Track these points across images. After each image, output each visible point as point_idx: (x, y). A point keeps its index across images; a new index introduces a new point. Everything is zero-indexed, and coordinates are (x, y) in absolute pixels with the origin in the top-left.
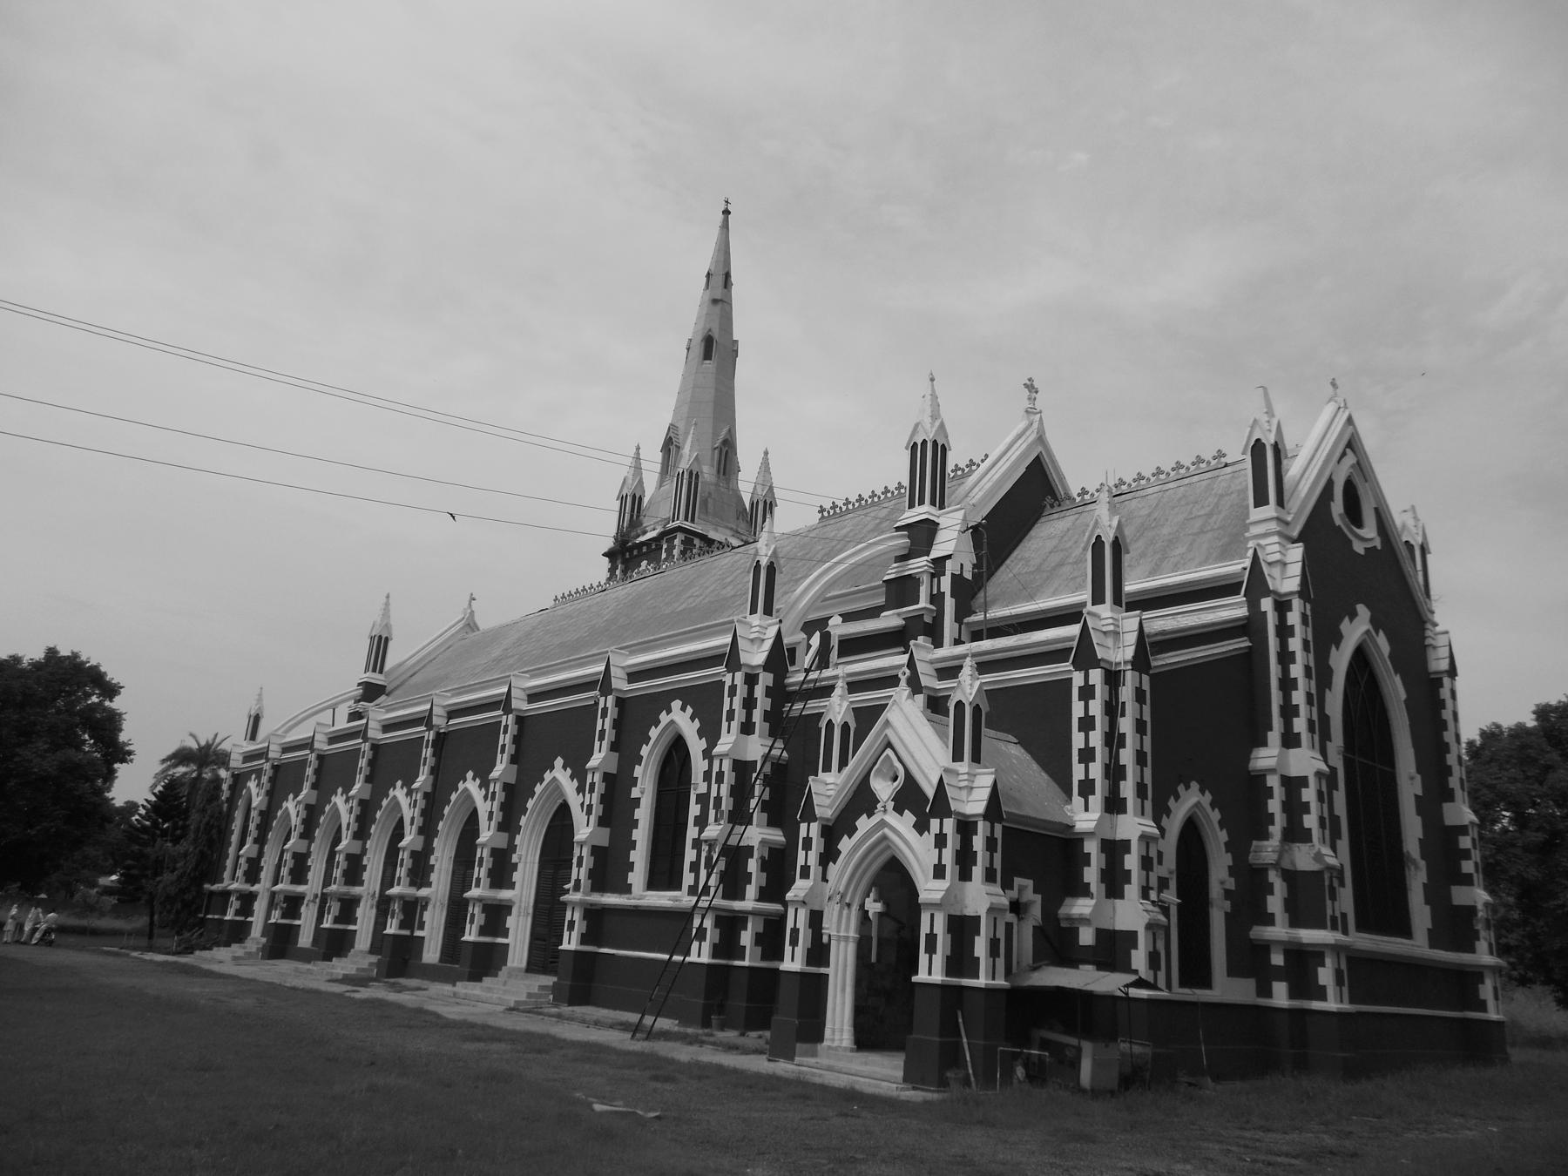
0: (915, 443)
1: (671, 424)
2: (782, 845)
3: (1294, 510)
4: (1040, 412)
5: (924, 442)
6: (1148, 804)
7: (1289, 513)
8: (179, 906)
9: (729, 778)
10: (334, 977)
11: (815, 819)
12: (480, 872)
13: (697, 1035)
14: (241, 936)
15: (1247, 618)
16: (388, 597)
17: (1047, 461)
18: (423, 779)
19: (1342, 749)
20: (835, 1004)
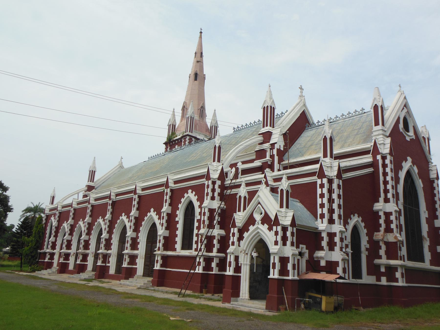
0: (265, 107)
1: (184, 102)
2: (224, 235)
3: (388, 127)
4: (304, 96)
5: (268, 106)
6: (342, 221)
7: (386, 128)
8: (30, 257)
9: (207, 214)
10: (81, 279)
11: (236, 227)
12: (128, 245)
13: (199, 295)
14: (50, 267)
15: (373, 162)
16: (95, 158)
17: (307, 112)
18: (108, 216)
19: (403, 203)
20: (243, 285)
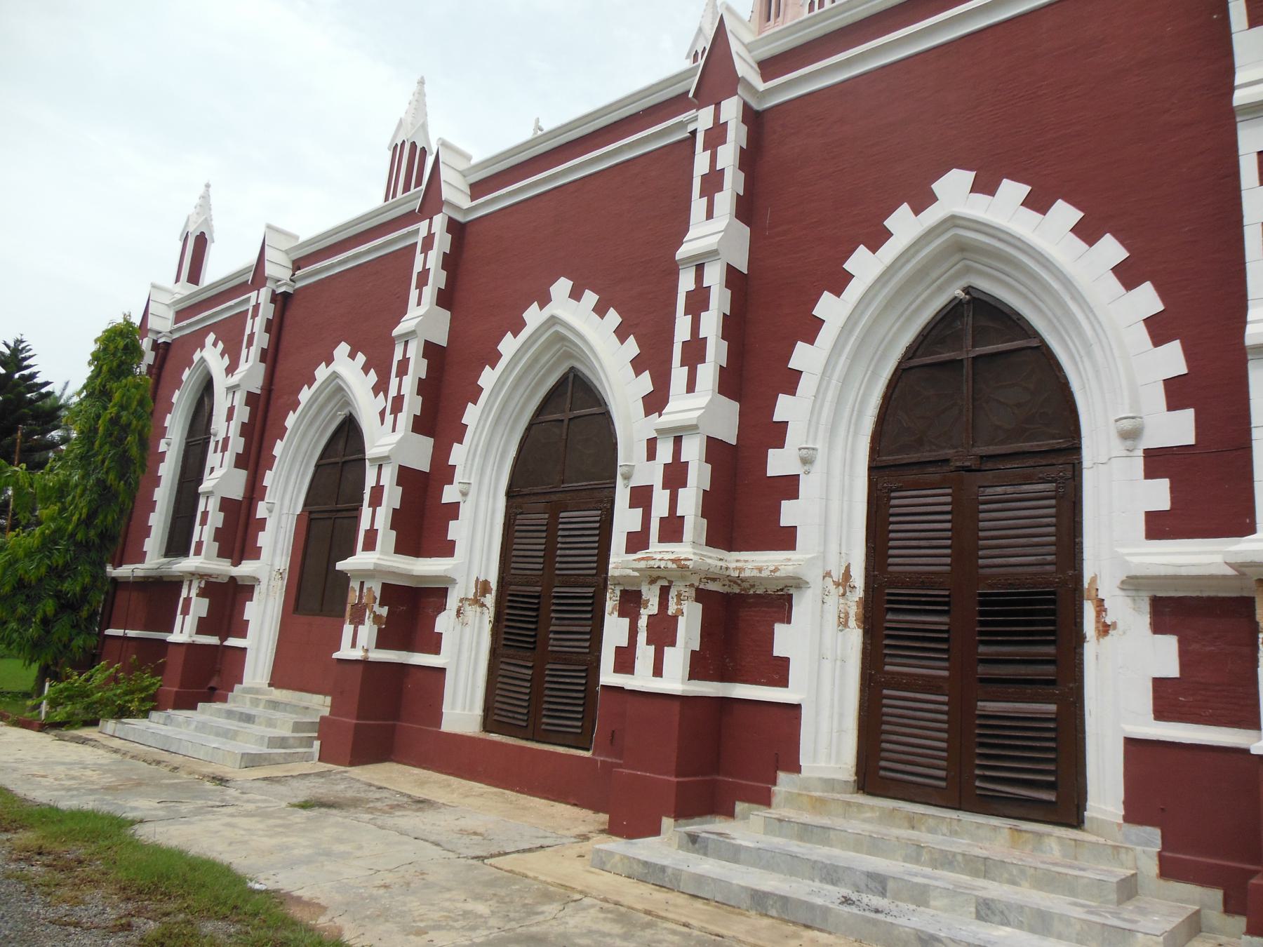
8: (49, 606)
14: (212, 684)
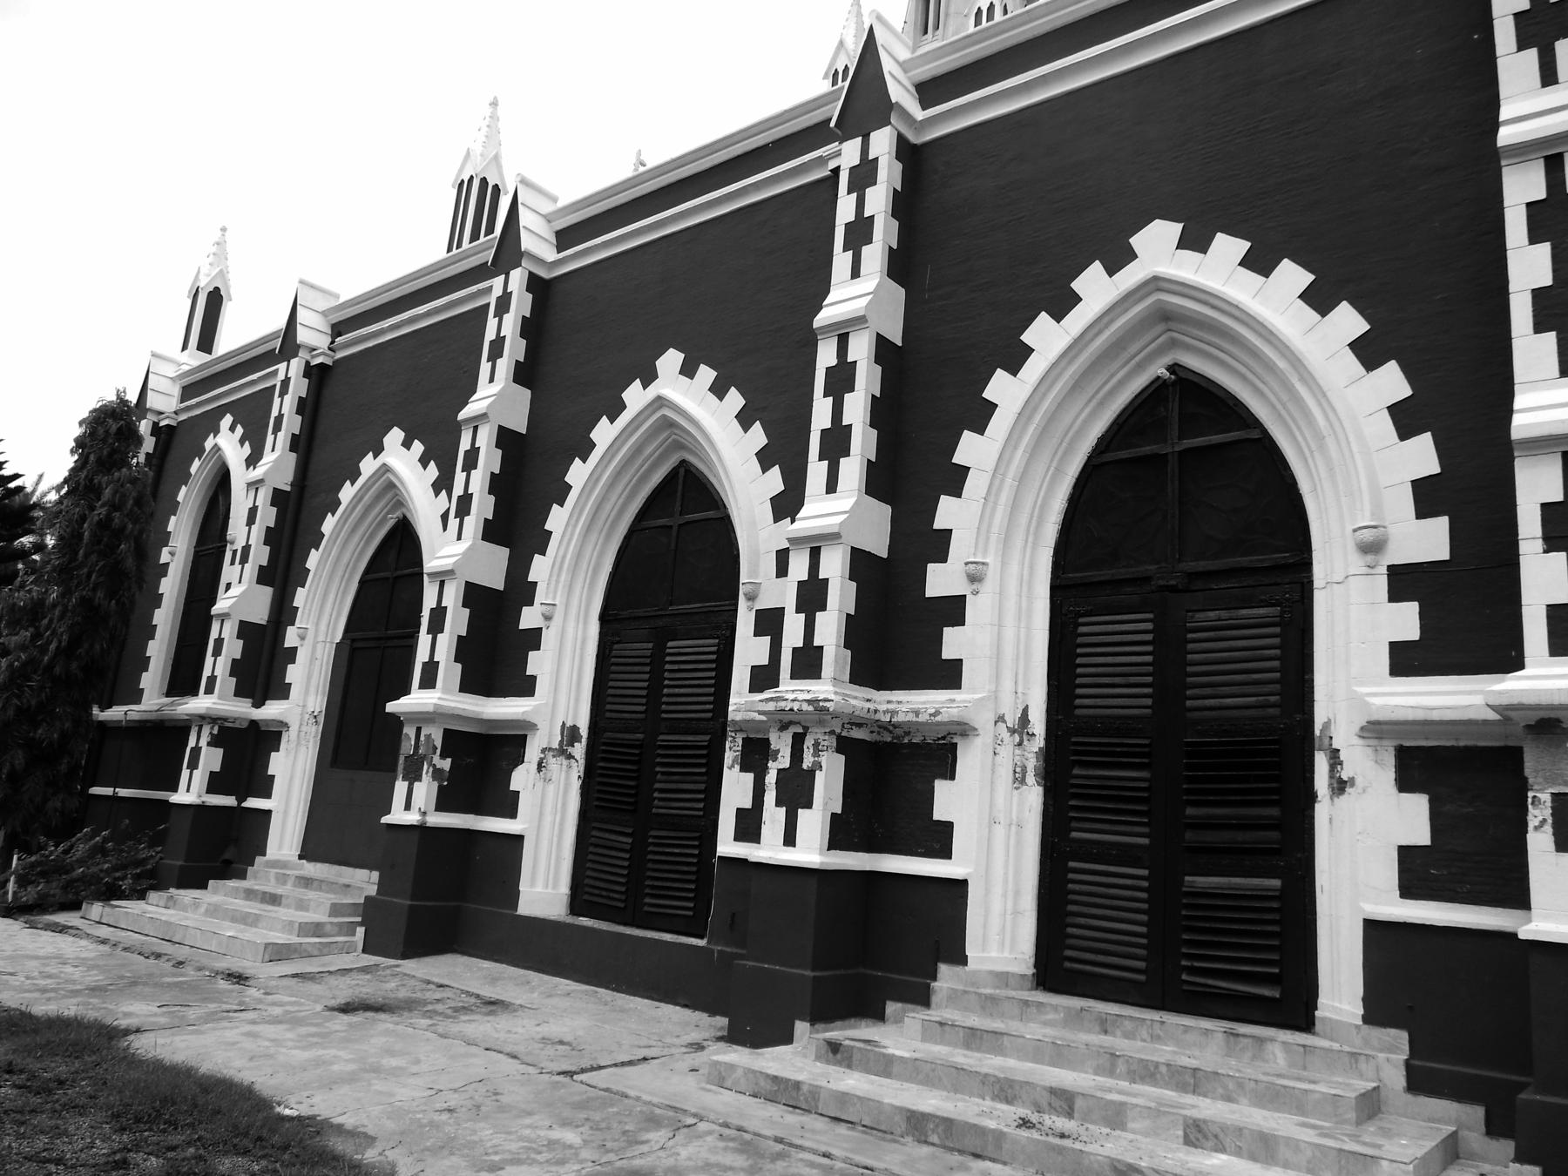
14: (227, 856)
